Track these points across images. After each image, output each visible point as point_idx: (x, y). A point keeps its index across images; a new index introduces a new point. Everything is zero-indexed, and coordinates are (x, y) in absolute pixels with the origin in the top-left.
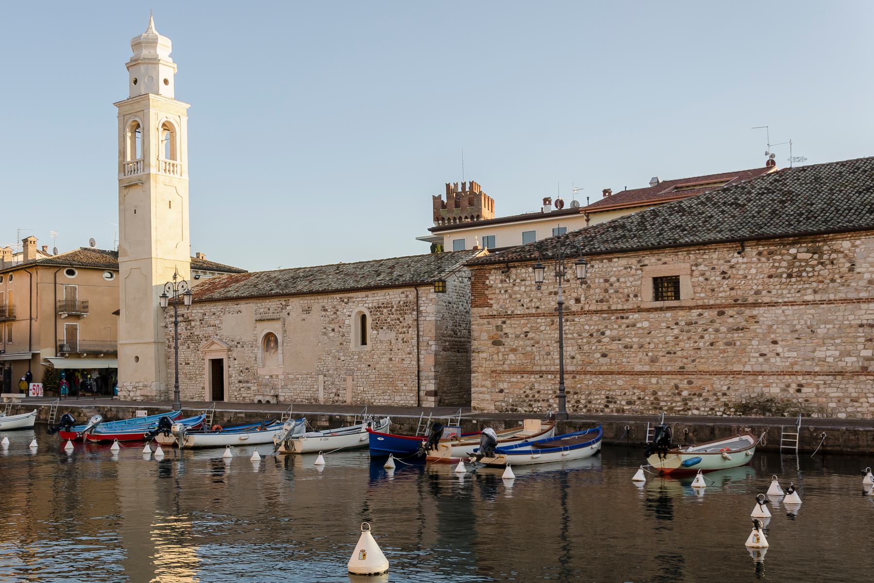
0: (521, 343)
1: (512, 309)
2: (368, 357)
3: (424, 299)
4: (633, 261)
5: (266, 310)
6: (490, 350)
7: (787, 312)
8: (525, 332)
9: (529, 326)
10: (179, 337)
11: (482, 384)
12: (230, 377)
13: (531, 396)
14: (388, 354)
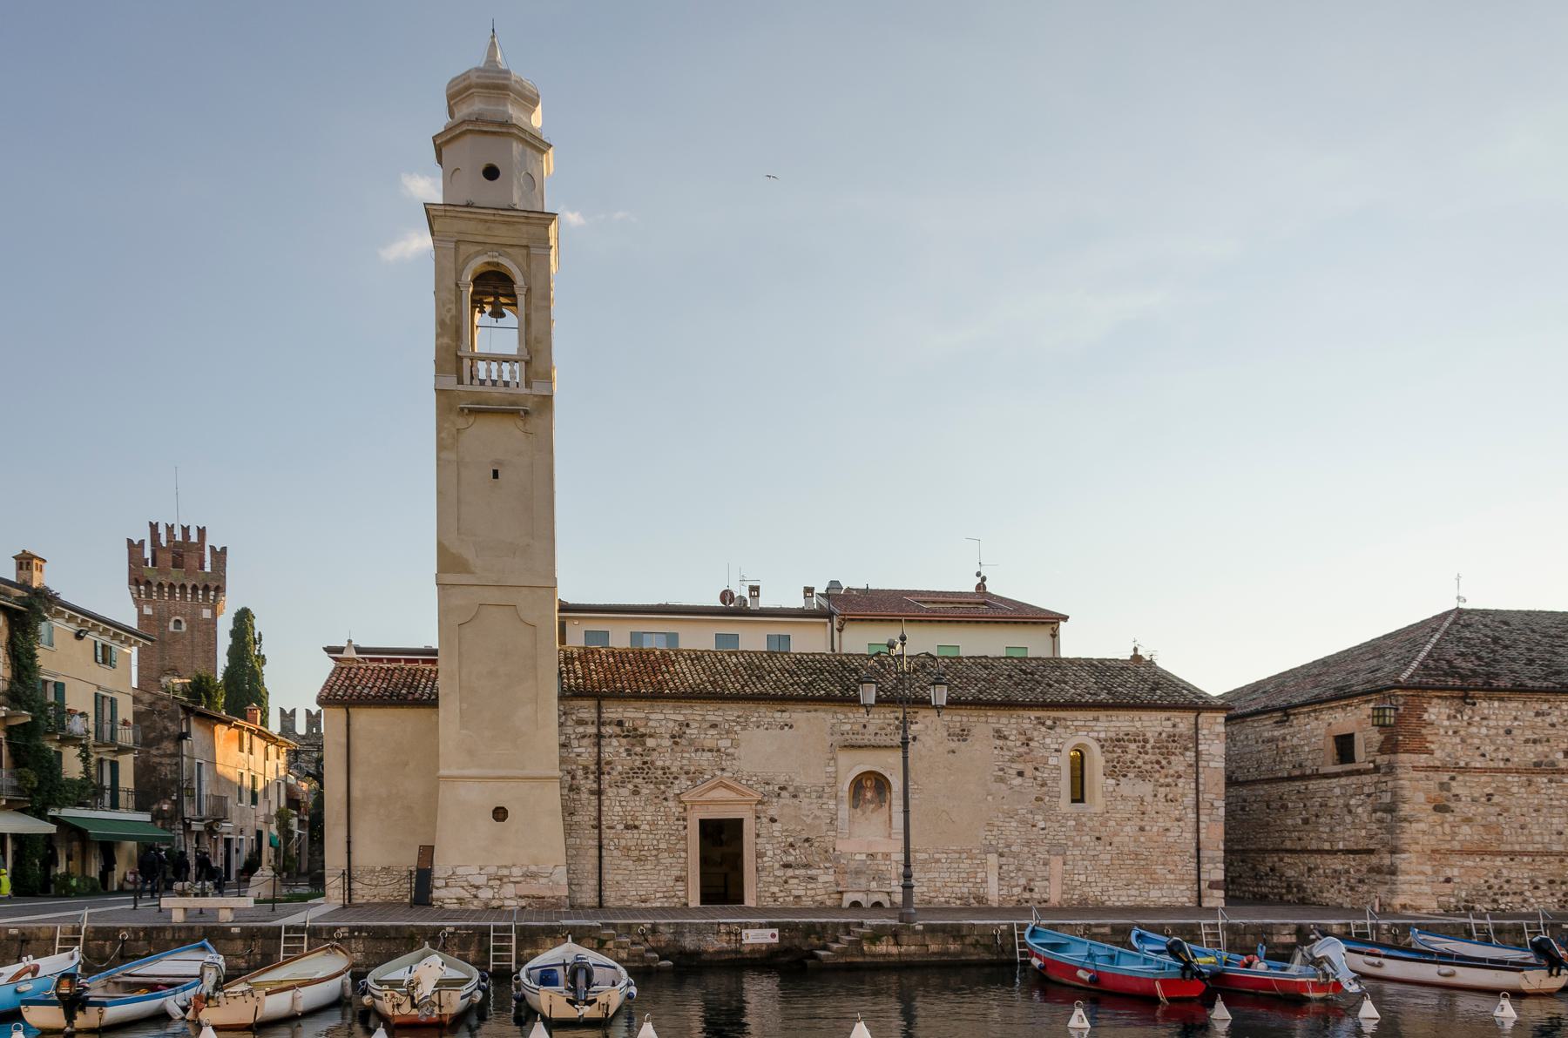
0: (1481, 810)
1: (1468, 760)
2: (1097, 824)
3: (1205, 732)
5: (856, 727)
6: (1431, 819)
8: (1488, 795)
9: (1494, 785)
10: (606, 769)
11: (1419, 870)
12: (760, 855)
13: (1497, 887)
14: (1138, 820)
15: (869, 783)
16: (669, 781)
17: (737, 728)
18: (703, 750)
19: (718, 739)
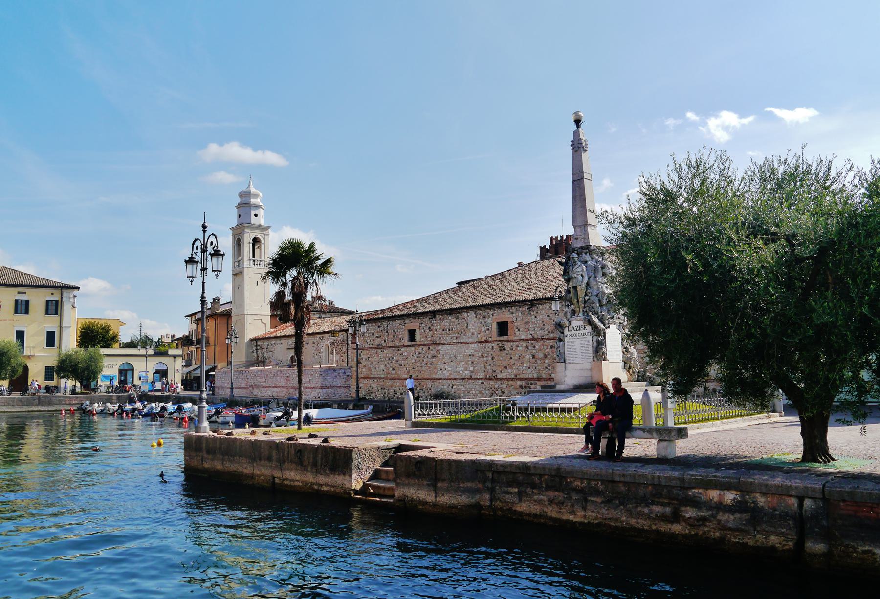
4: (402, 321)
7: (449, 348)
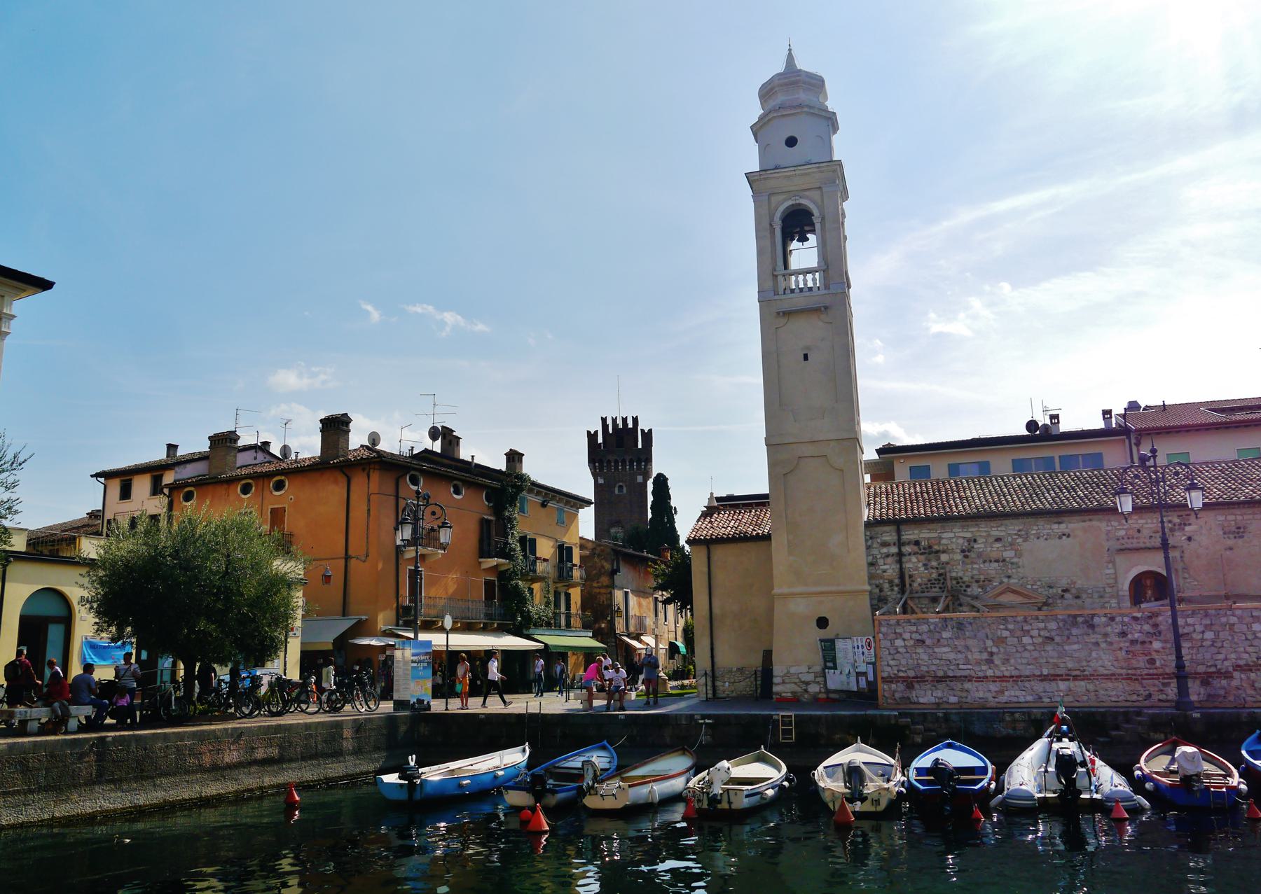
15: (1148, 582)
16: (962, 589)
17: (1020, 540)
18: (991, 561)
19: (1002, 551)
